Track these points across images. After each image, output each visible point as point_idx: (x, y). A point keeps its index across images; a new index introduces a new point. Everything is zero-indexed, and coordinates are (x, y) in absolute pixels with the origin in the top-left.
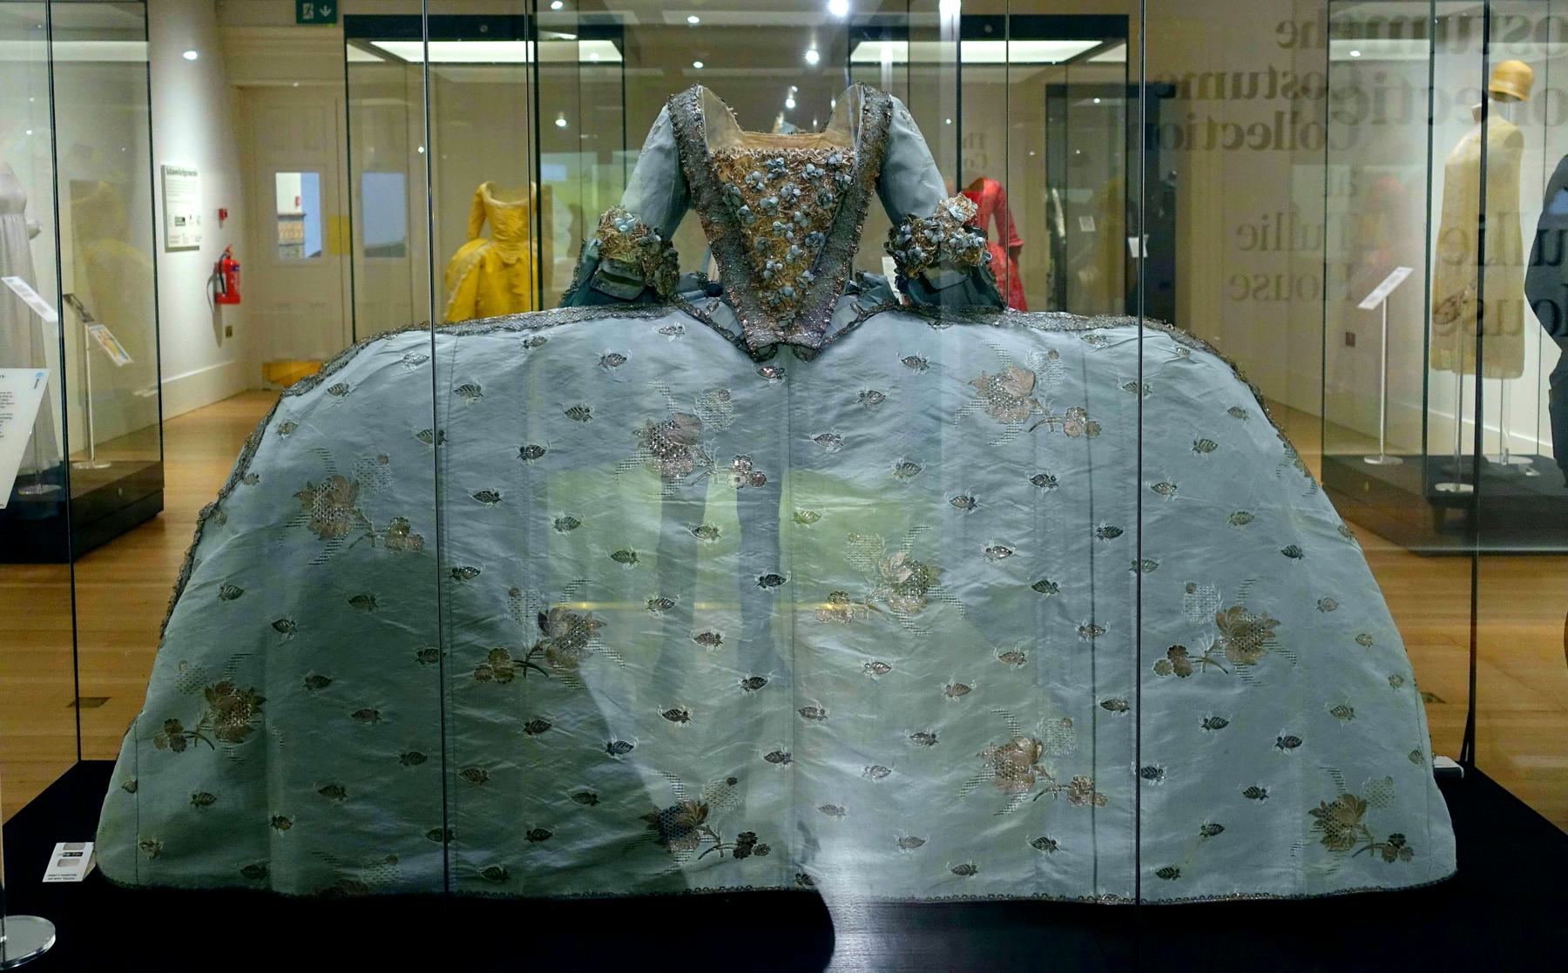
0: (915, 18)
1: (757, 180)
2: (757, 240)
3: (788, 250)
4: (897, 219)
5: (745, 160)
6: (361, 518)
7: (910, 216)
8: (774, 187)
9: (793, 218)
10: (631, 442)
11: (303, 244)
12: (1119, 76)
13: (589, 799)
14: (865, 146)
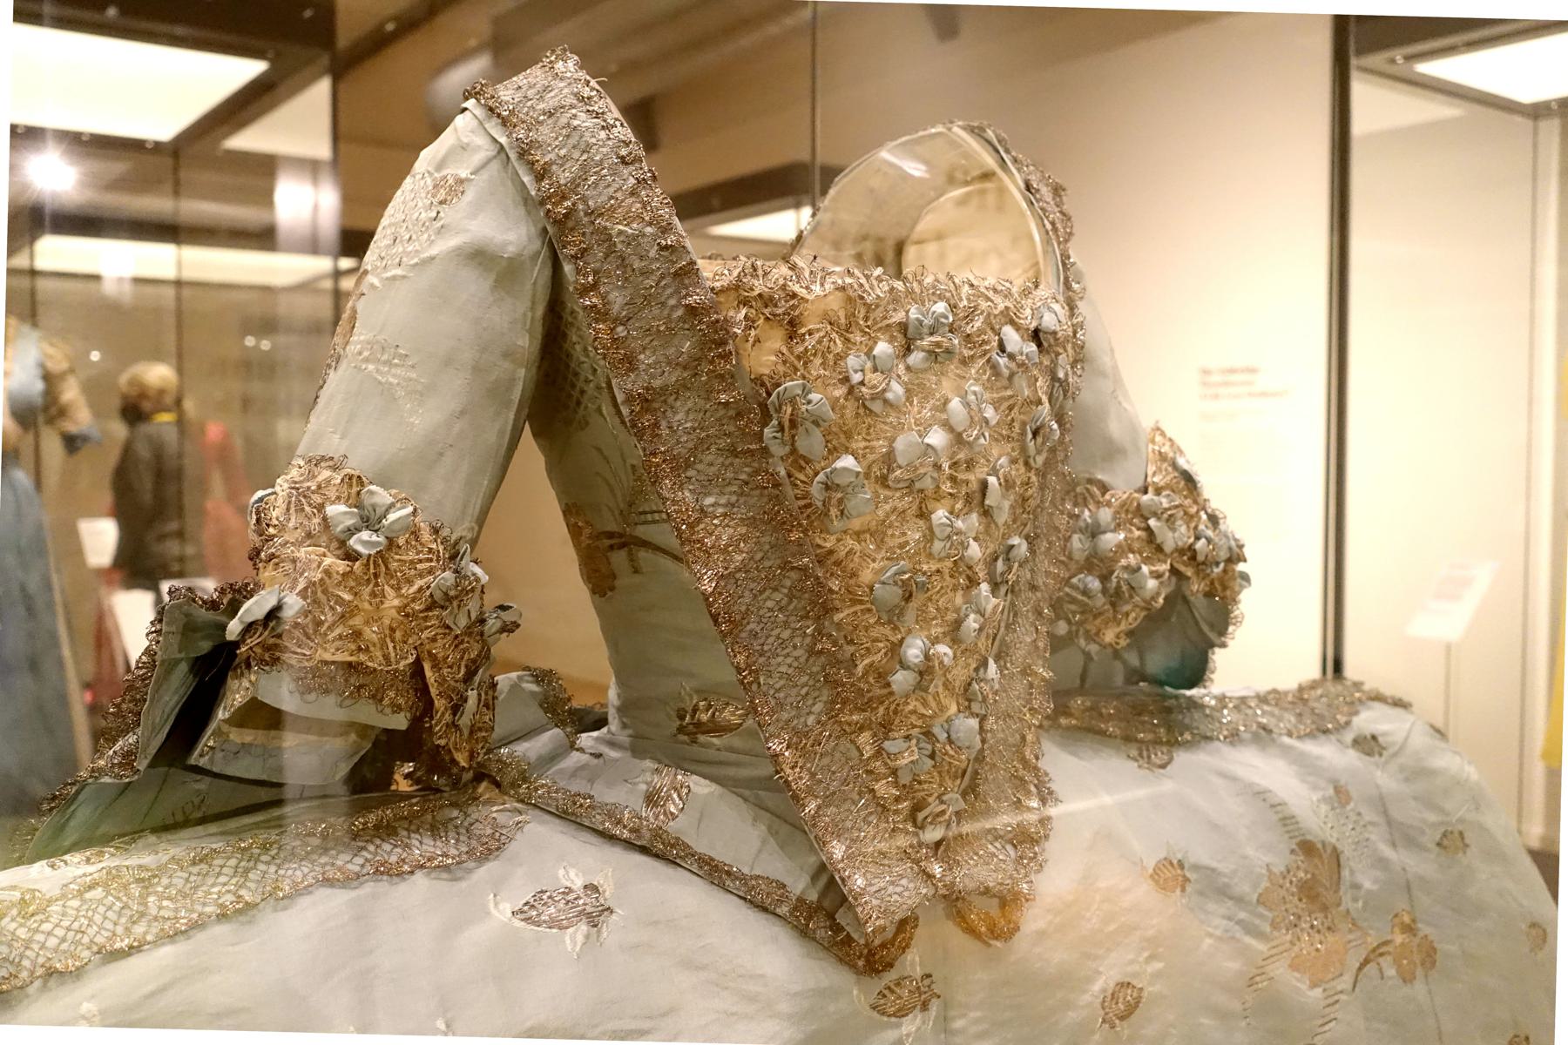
7: (1090, 481)
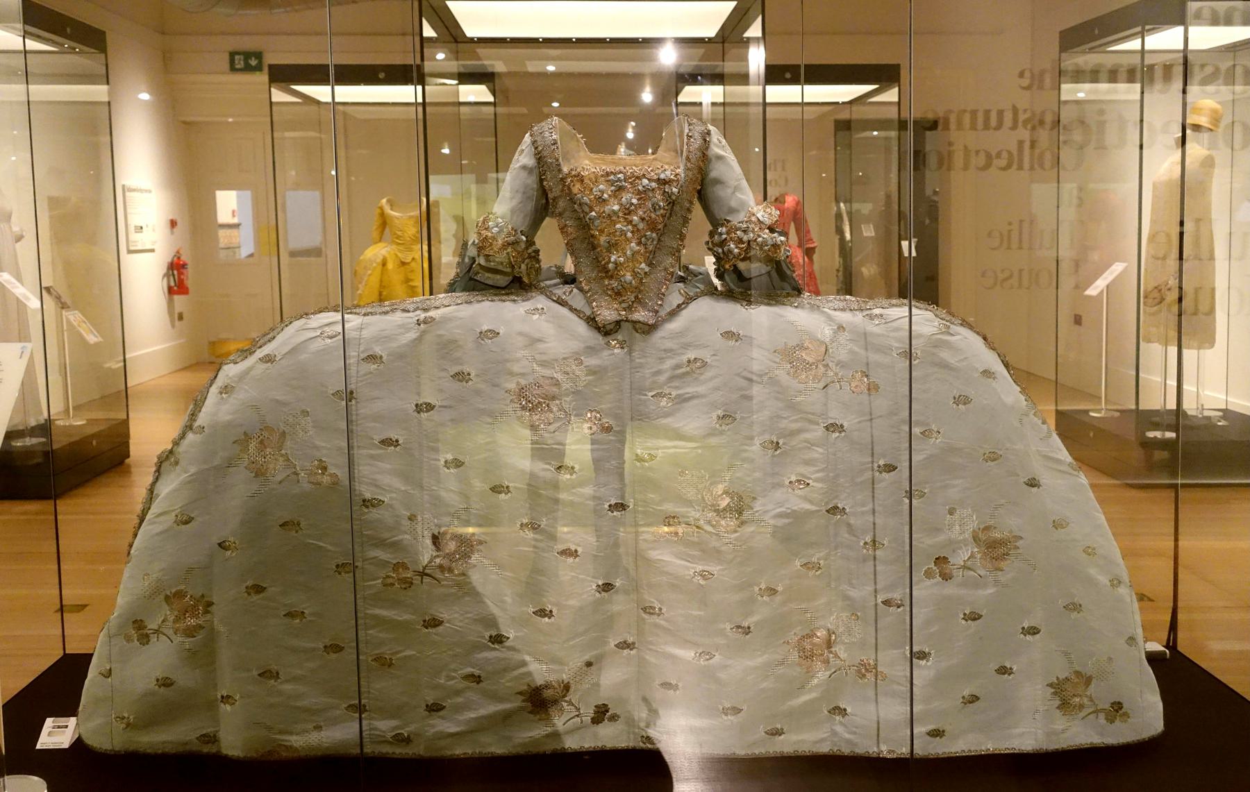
0: (729, 67)
1: (602, 192)
2: (603, 239)
3: (628, 247)
4: (715, 222)
5: (592, 176)
6: (288, 460)
8: (616, 197)
9: (631, 221)
11: (239, 247)
12: (893, 113)
14: (689, 164)
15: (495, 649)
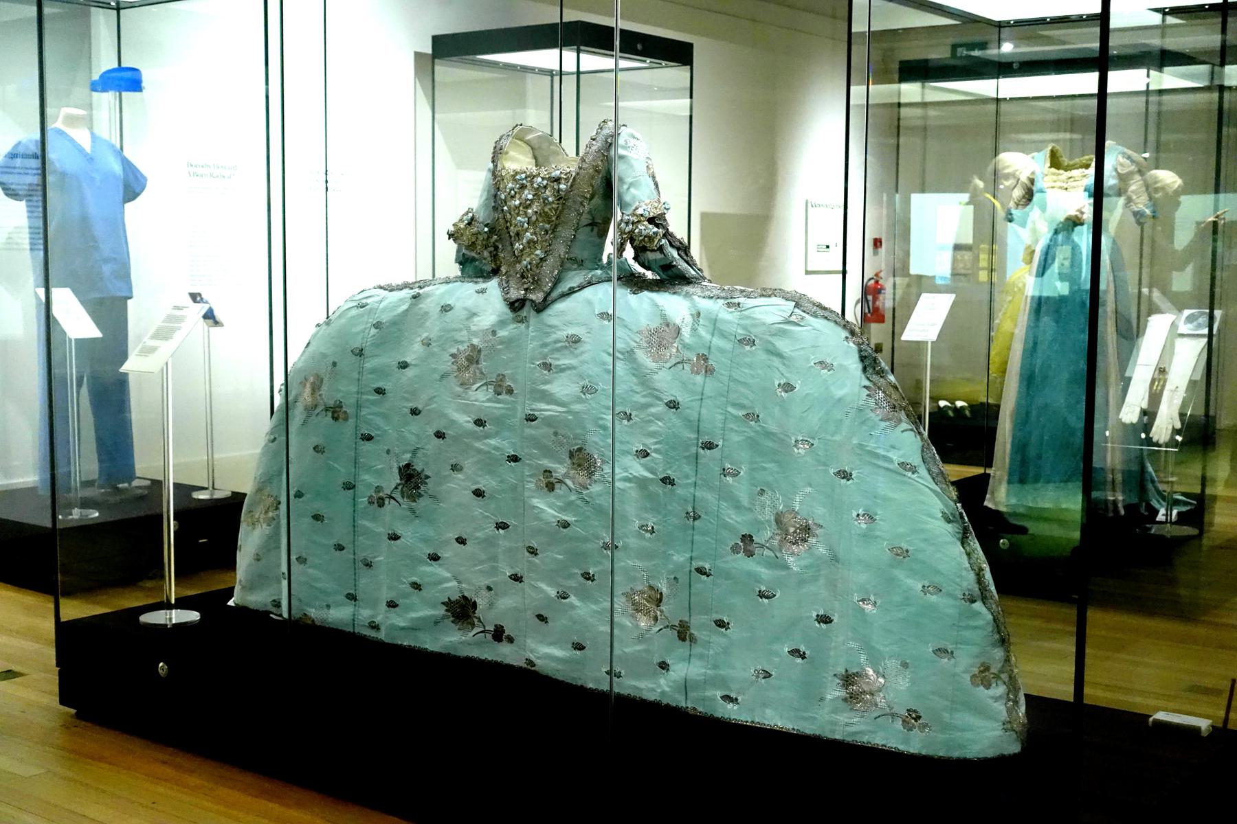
10: (448, 361)
13: (417, 586)
15: (432, 565)
